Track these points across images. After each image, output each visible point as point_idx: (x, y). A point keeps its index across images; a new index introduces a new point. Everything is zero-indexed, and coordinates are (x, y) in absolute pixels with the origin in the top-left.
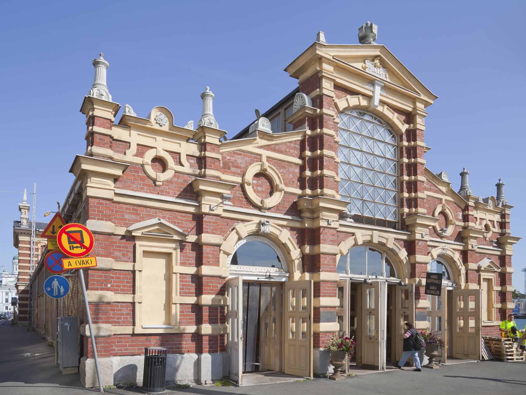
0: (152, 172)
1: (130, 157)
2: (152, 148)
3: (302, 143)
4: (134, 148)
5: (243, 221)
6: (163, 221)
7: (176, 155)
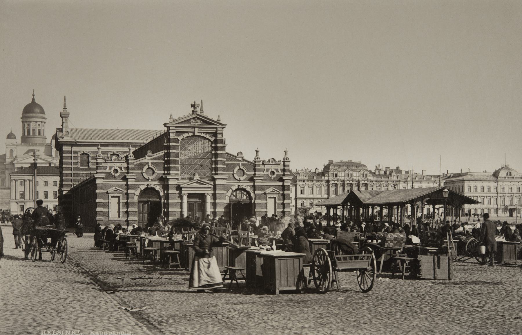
0: (113, 174)
1: (108, 170)
3: (164, 155)
4: (108, 168)
7: (120, 168)
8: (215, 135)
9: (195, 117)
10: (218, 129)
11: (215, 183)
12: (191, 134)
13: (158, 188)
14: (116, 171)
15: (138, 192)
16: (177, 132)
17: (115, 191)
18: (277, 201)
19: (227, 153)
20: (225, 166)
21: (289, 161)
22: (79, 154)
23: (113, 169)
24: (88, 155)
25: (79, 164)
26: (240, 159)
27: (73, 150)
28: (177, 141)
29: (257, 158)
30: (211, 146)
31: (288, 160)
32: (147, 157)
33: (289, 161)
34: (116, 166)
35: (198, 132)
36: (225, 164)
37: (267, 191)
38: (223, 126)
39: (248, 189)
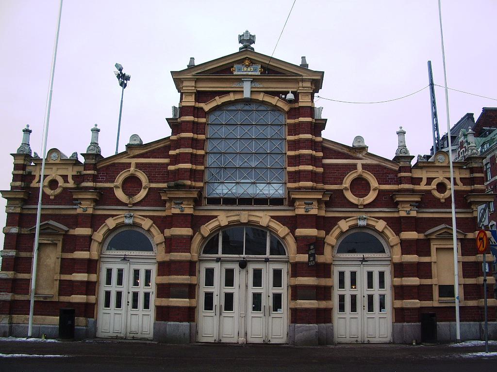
2: (48, 175)
5: (113, 216)
7: (65, 178)
12: (231, 97)
14: (53, 184)
15: (99, 236)
19: (323, 138)
20: (321, 170)
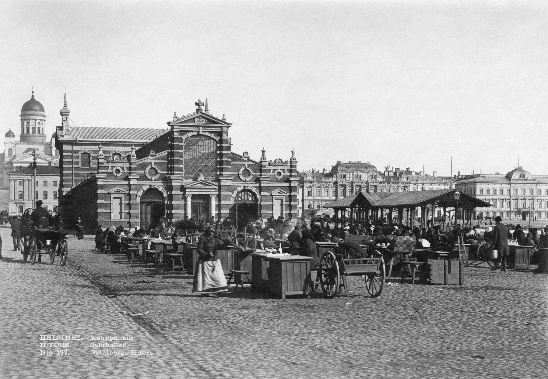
0: (115, 174)
1: (109, 170)
3: (168, 155)
6: (119, 188)
7: (122, 168)
8: (220, 134)
9: (200, 116)
10: (223, 128)
11: (219, 183)
12: (195, 133)
13: (161, 189)
14: (118, 171)
15: (140, 193)
16: (180, 131)
17: (117, 191)
18: (284, 203)
19: (232, 153)
20: (230, 167)
21: (297, 162)
22: (80, 154)
23: (115, 169)
24: (89, 154)
25: (80, 163)
26: (246, 159)
27: (73, 149)
28: (181, 140)
29: (263, 159)
30: (216, 146)
31: (295, 161)
32: (150, 157)
33: (297, 162)
34: (118, 166)
35: (203, 132)
36: (230, 165)
37: (274, 193)
38: (229, 125)
39: (254, 190)
